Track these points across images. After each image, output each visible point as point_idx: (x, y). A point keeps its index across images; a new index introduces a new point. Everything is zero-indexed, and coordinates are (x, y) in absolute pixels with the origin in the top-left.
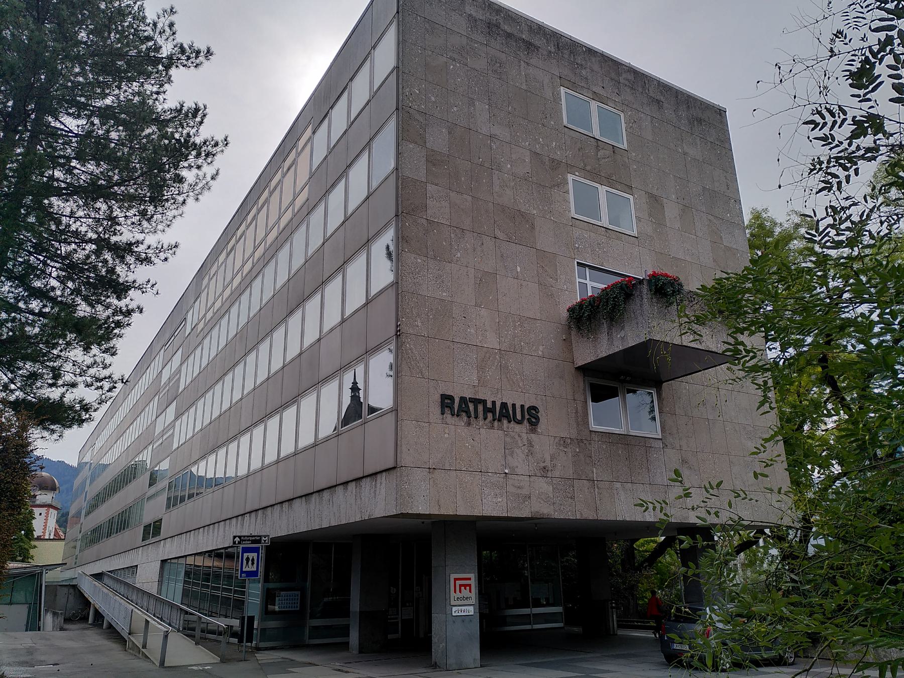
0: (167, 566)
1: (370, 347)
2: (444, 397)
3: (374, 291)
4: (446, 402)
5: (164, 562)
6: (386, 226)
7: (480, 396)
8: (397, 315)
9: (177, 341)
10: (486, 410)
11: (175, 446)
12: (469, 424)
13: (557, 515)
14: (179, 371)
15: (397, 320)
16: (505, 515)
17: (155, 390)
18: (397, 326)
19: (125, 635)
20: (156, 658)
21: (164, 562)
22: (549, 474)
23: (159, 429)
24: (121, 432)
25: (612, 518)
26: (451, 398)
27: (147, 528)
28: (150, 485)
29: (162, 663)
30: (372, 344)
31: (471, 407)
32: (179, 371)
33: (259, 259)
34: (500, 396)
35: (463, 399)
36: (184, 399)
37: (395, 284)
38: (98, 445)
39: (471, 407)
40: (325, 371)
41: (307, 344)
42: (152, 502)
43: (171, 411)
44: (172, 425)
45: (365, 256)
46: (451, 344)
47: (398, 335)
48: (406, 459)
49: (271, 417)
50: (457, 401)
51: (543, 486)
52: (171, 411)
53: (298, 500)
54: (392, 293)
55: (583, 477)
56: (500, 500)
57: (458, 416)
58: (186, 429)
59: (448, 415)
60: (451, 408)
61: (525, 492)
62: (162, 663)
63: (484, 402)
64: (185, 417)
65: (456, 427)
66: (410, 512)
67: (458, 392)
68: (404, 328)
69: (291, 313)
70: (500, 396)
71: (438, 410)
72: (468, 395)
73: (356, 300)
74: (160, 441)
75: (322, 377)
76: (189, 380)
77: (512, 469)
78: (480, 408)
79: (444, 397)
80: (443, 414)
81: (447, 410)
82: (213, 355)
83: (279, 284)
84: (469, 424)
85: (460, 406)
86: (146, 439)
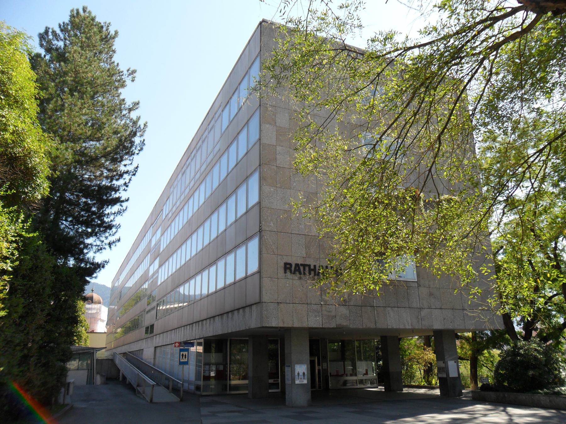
0: (158, 350)
1: (248, 236)
2: (286, 264)
3: (250, 205)
4: (287, 267)
5: (155, 347)
6: (255, 170)
7: (307, 263)
8: (260, 220)
9: (159, 222)
10: (310, 270)
11: (159, 283)
12: (300, 278)
13: (351, 326)
14: (160, 240)
15: (260, 223)
16: (321, 326)
17: (148, 251)
18: (260, 226)
19: (135, 386)
20: (148, 399)
21: (155, 347)
22: (347, 304)
23: (151, 273)
24: (132, 273)
25: (384, 327)
26: (290, 264)
27: (147, 328)
28: (148, 305)
29: (151, 401)
30: (249, 235)
31: (302, 268)
32: (160, 240)
33: (197, 180)
34: (318, 262)
35: (297, 265)
36: (164, 257)
37: (259, 203)
38: (121, 281)
39: (302, 268)
40: (229, 248)
41: (220, 232)
42: (149, 314)
43: (157, 262)
44: (157, 271)
45: (245, 186)
46: (290, 235)
47: (260, 231)
48: (265, 298)
49: (204, 271)
50: (293, 266)
51: (344, 310)
52: (157, 262)
53: (217, 317)
54: (257, 208)
55: (368, 305)
56: (318, 318)
57: (294, 273)
58: (164, 275)
59: (288, 273)
60: (290, 269)
61: (333, 314)
62: (151, 401)
63: (309, 266)
64: (163, 267)
65: (293, 281)
66: (267, 326)
67: (294, 260)
68: (264, 228)
69: (213, 213)
70: (318, 262)
71: (283, 271)
72: (300, 262)
73: (242, 210)
74: (152, 280)
75: (227, 251)
76: (165, 246)
77: (325, 301)
78: (307, 269)
79: (286, 264)
80: (285, 272)
81: (288, 271)
82: (172, 238)
83: (195, 211)
84: (300, 278)
85: (295, 268)
86: (144, 278)
